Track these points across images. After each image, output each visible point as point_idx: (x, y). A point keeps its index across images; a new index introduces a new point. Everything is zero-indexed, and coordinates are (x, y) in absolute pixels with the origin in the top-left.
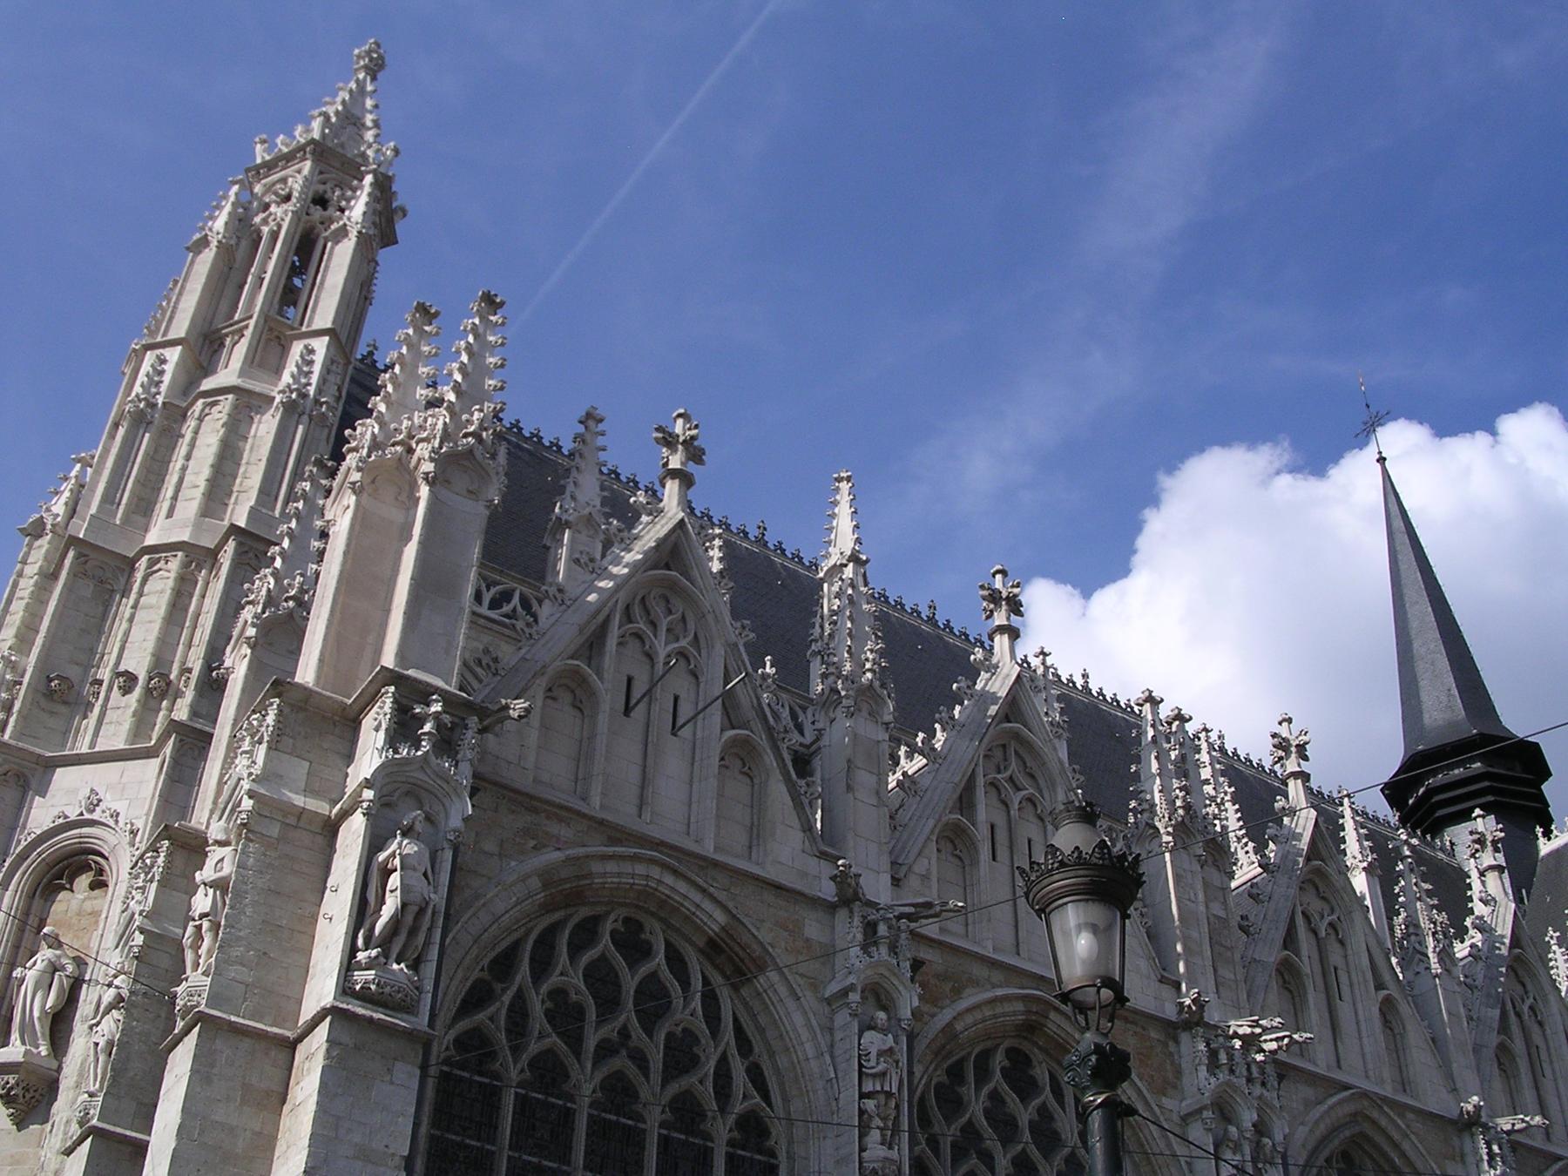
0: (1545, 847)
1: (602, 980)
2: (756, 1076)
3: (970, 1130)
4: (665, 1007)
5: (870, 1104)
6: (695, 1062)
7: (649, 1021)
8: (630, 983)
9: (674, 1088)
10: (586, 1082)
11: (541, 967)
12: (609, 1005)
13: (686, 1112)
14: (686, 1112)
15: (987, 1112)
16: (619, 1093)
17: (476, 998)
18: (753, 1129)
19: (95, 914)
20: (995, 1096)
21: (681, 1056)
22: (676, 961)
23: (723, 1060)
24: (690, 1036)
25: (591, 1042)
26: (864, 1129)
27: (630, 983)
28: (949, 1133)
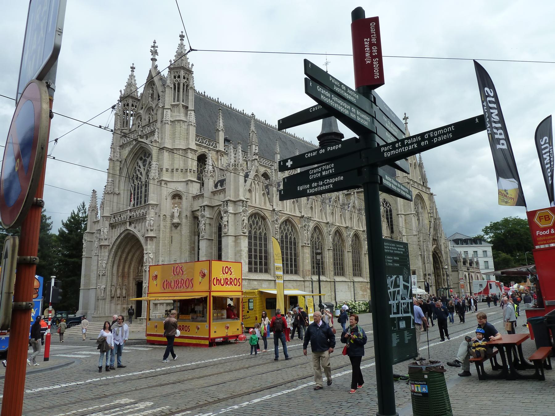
1: (253, 222)
3: (282, 231)
5: (276, 232)
7: (257, 225)
9: (259, 231)
12: (254, 224)
13: (260, 233)
24: (260, 225)
25: (253, 229)
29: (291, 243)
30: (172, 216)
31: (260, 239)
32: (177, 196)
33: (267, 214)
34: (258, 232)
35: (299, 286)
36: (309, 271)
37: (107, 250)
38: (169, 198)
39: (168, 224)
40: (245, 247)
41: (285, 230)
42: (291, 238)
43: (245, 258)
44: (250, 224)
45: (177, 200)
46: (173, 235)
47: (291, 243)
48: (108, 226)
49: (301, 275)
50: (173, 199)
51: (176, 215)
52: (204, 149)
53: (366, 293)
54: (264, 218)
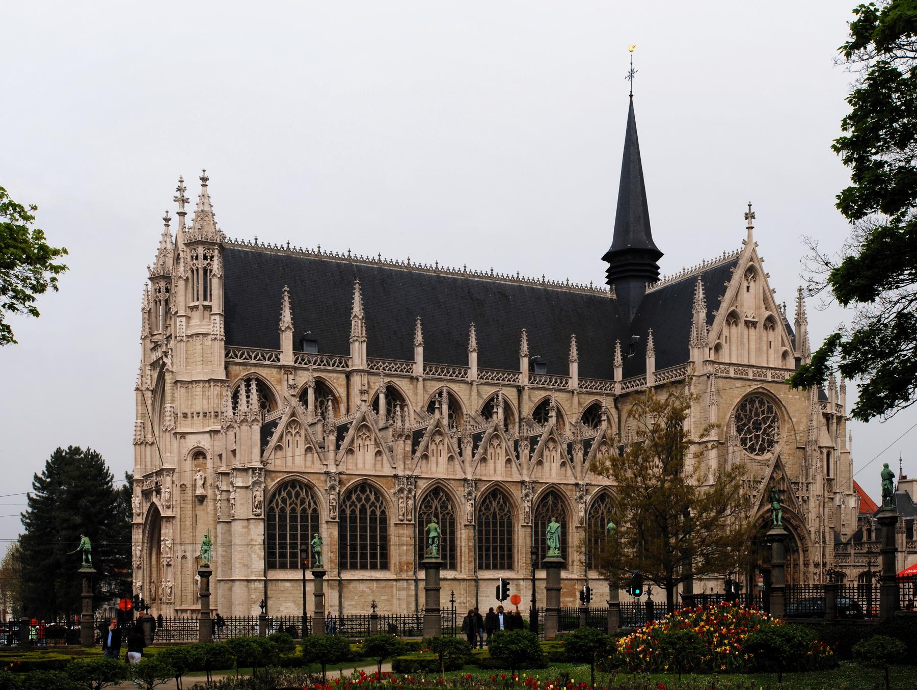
0: (648, 291)
1: (289, 494)
2: (315, 503)
3: (353, 502)
4: (299, 495)
6: (305, 502)
8: (293, 494)
10: (288, 510)
11: (279, 495)
12: (290, 498)
13: (304, 510)
14: (304, 510)
15: (356, 498)
16: (293, 510)
17: (271, 502)
18: (315, 510)
19: (206, 464)
20: (358, 495)
21: (303, 502)
22: (301, 488)
23: (309, 501)
24: (304, 498)
26: (330, 510)
27: (293, 494)
28: (348, 504)
29: (373, 520)
30: (194, 486)
31: (304, 518)
32: (199, 454)
33: (313, 480)
34: (299, 509)
35: (383, 587)
36: (408, 564)
37: (141, 531)
38: (189, 459)
39: (189, 496)
40: (258, 535)
41: (359, 499)
42: (373, 512)
43: (258, 551)
44: (283, 498)
45: (201, 460)
46: (197, 512)
47: (373, 520)
48: (140, 494)
49: (393, 571)
50: (195, 459)
51: (200, 483)
52: (253, 368)
53: (572, 599)
54: (309, 487)
